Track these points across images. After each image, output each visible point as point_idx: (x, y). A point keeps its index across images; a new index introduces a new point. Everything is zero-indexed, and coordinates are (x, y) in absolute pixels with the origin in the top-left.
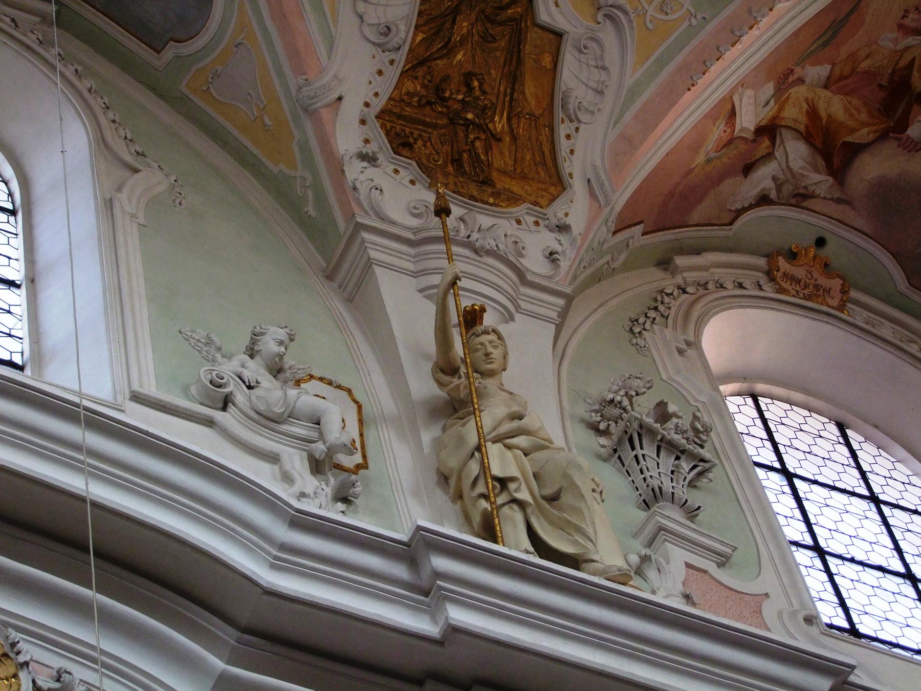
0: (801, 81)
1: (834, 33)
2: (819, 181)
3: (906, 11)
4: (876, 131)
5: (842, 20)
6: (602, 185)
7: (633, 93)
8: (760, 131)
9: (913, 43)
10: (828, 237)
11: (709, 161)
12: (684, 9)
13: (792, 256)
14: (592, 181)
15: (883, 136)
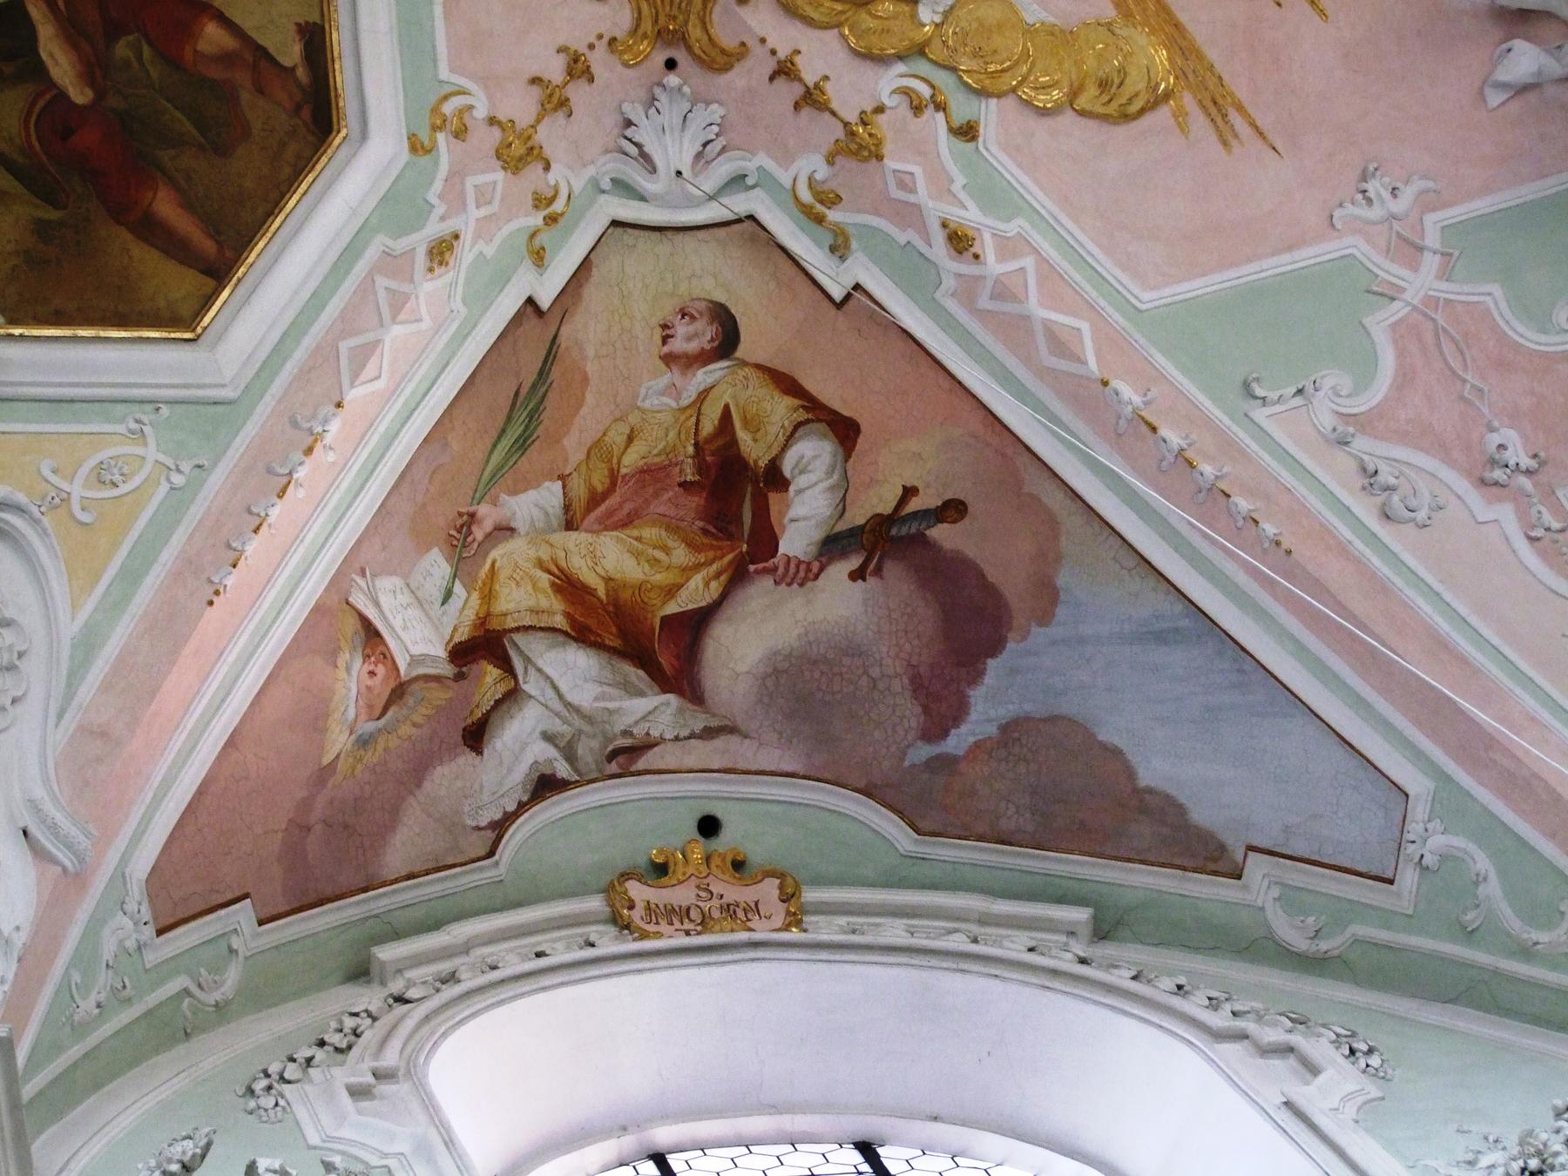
0: (505, 530)
1: (531, 417)
2: (648, 709)
3: (665, 327)
4: (718, 575)
5: (534, 386)
6: (53, 828)
7: (87, 644)
8: (461, 655)
9: (710, 380)
10: (718, 810)
11: (364, 742)
12: (148, 467)
13: (660, 870)
14: (34, 830)
15: (738, 577)
